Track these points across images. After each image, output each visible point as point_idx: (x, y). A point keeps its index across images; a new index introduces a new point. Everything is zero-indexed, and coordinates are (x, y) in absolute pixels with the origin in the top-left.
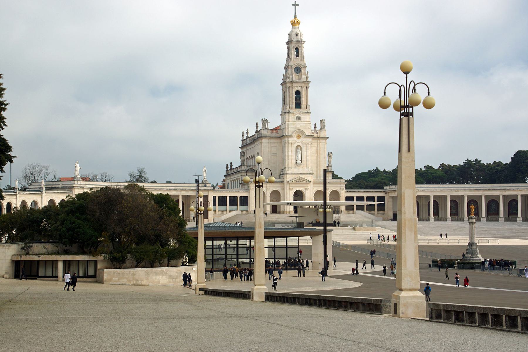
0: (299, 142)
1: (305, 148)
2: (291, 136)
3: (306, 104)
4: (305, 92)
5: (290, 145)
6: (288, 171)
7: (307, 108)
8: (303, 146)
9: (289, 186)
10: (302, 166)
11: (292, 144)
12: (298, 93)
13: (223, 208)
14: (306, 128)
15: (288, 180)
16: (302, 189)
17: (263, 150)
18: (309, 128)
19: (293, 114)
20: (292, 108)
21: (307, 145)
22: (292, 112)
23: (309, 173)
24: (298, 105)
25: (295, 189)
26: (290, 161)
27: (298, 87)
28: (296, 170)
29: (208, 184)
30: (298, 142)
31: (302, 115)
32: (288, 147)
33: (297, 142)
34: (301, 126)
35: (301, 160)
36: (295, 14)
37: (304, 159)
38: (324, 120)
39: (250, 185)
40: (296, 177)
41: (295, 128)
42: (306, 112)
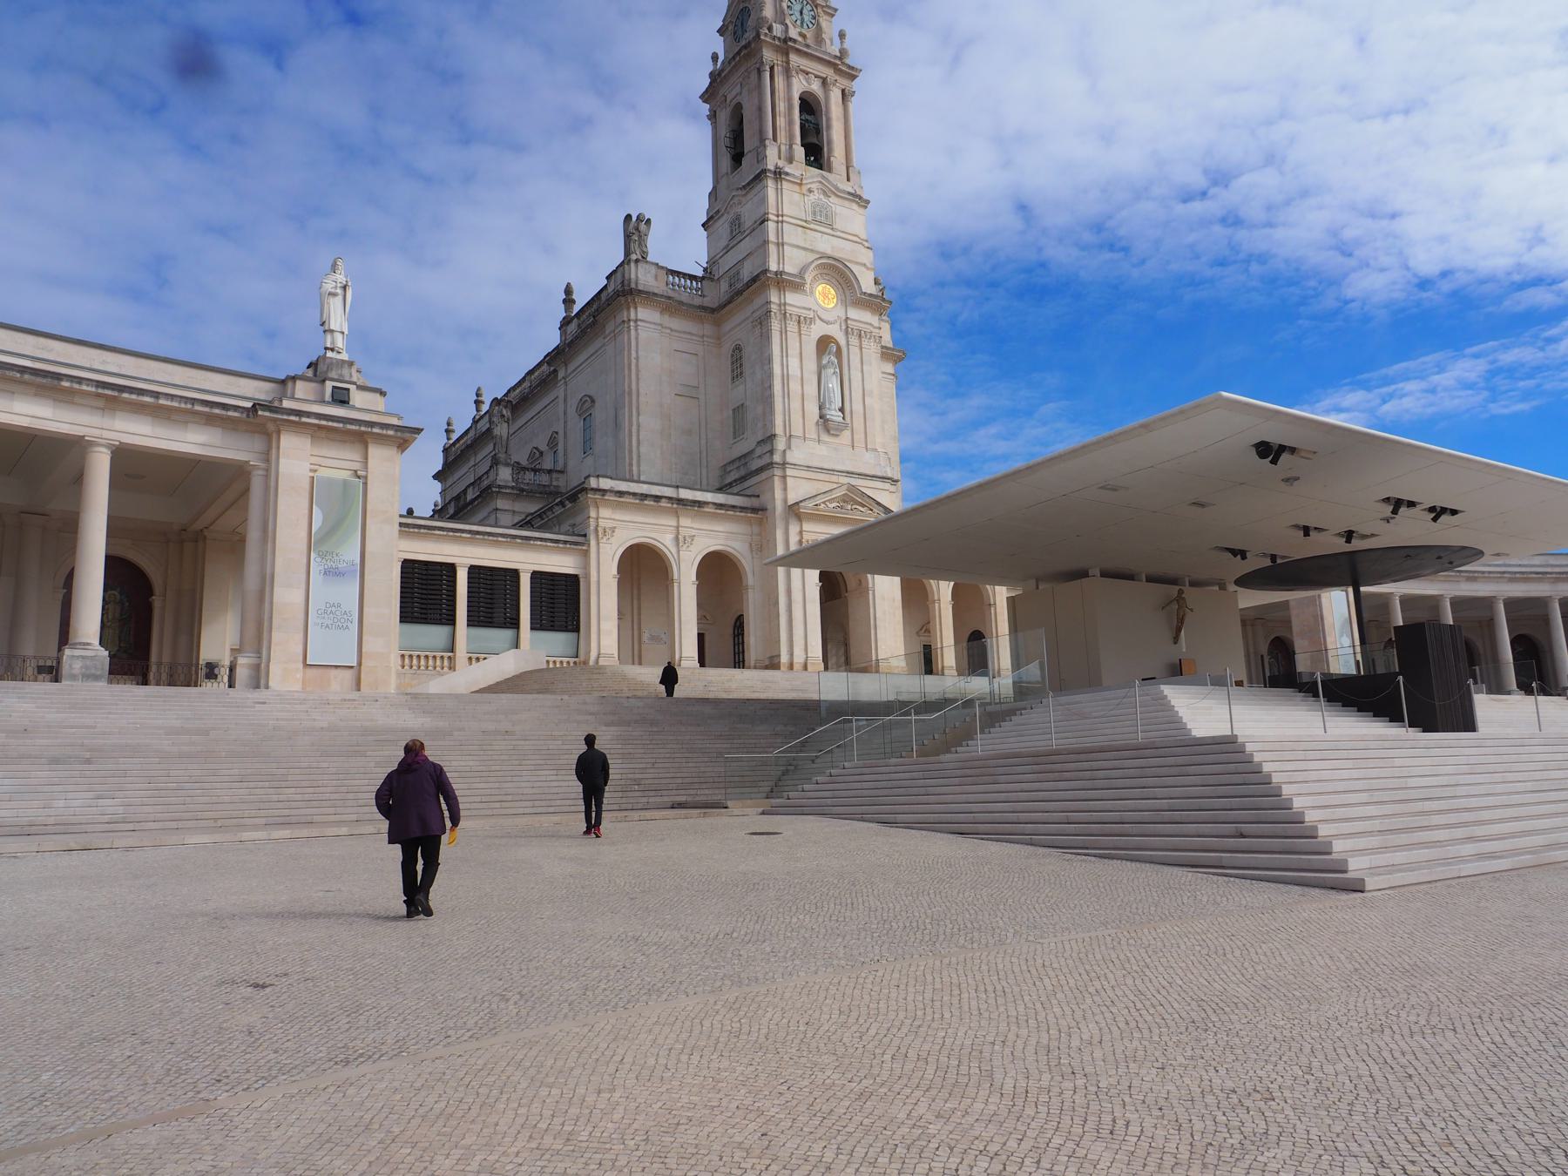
1: (855, 351)
2: (796, 285)
5: (792, 326)
6: (788, 452)
8: (848, 342)
9: (798, 529)
11: (799, 322)
12: (809, 106)
13: (433, 635)
15: (792, 500)
17: (637, 358)
18: (868, 269)
19: (797, 188)
20: (790, 160)
23: (879, 474)
24: (816, 154)
26: (795, 405)
28: (822, 450)
29: (361, 388)
30: (823, 317)
31: (833, 199)
32: (784, 332)
33: (820, 319)
34: (833, 248)
37: (858, 407)
39: (593, 514)
40: (828, 487)
41: (812, 251)
42: (849, 193)
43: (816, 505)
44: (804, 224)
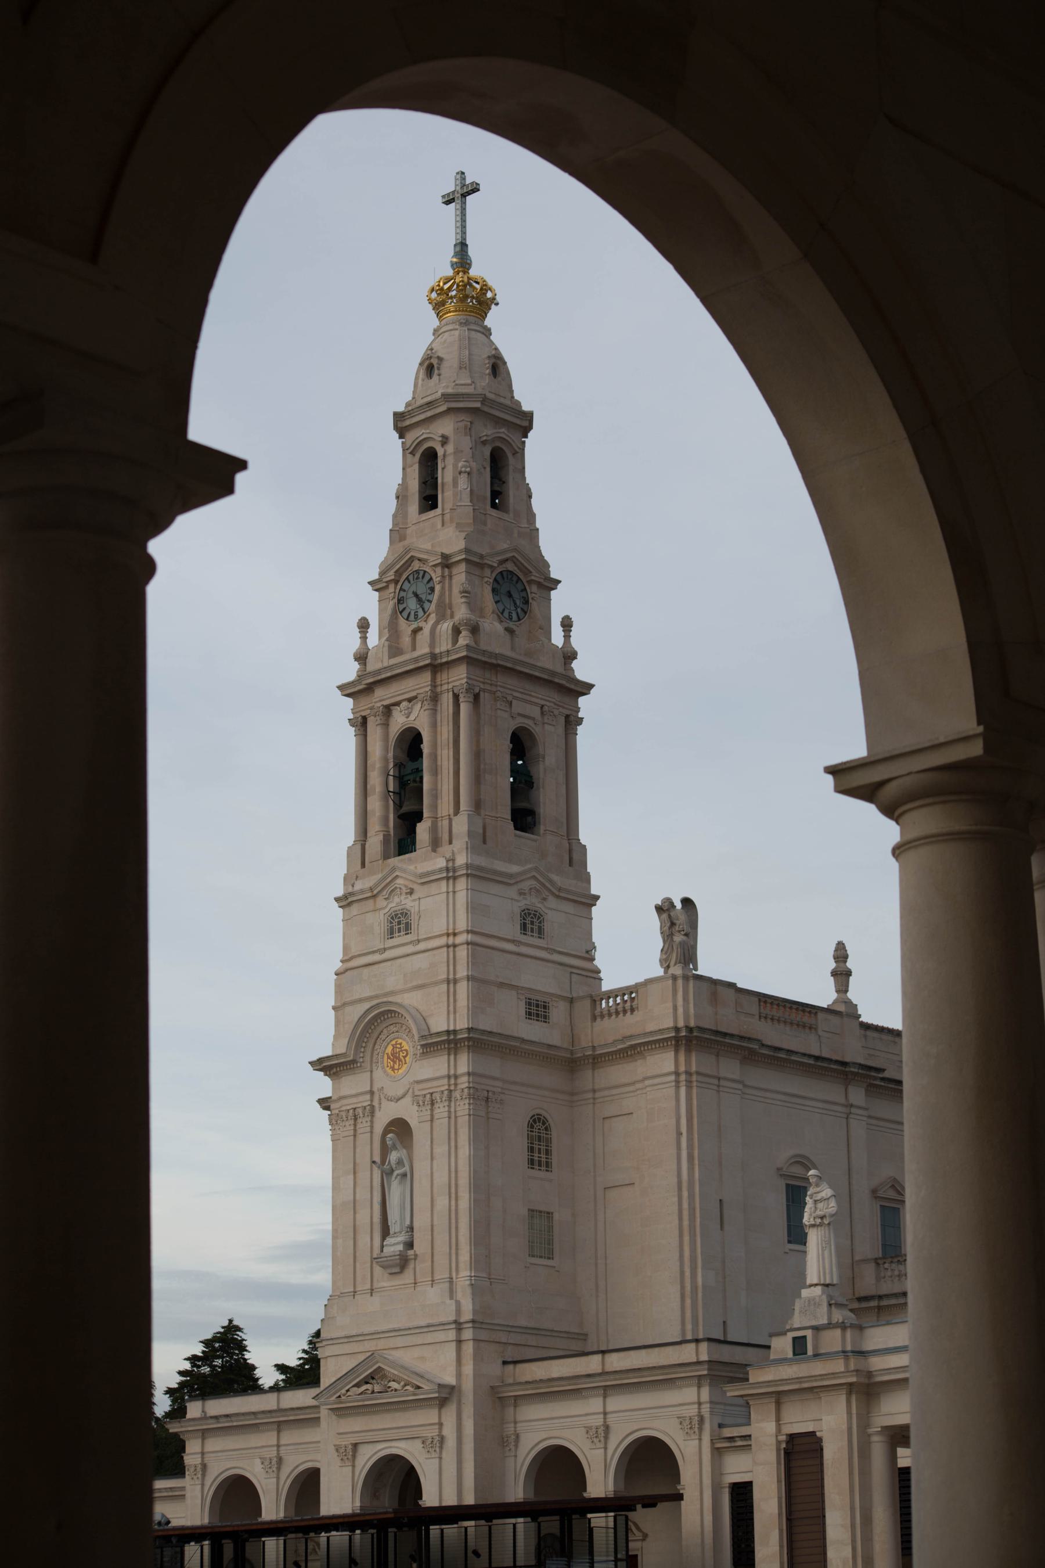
0: (400, 1093)
3: (452, 811)
4: (445, 732)
7: (450, 842)
10: (408, 1277)
14: (436, 983)
16: (402, 1444)
19: (371, 902)
21: (441, 1110)
22: (362, 891)
25: (370, 1446)
27: (404, 704)
28: (374, 1304)
30: (391, 1093)
35: (411, 1228)
36: (462, 247)
38: (687, 902)
43: (339, 1397)
44: (377, 957)
